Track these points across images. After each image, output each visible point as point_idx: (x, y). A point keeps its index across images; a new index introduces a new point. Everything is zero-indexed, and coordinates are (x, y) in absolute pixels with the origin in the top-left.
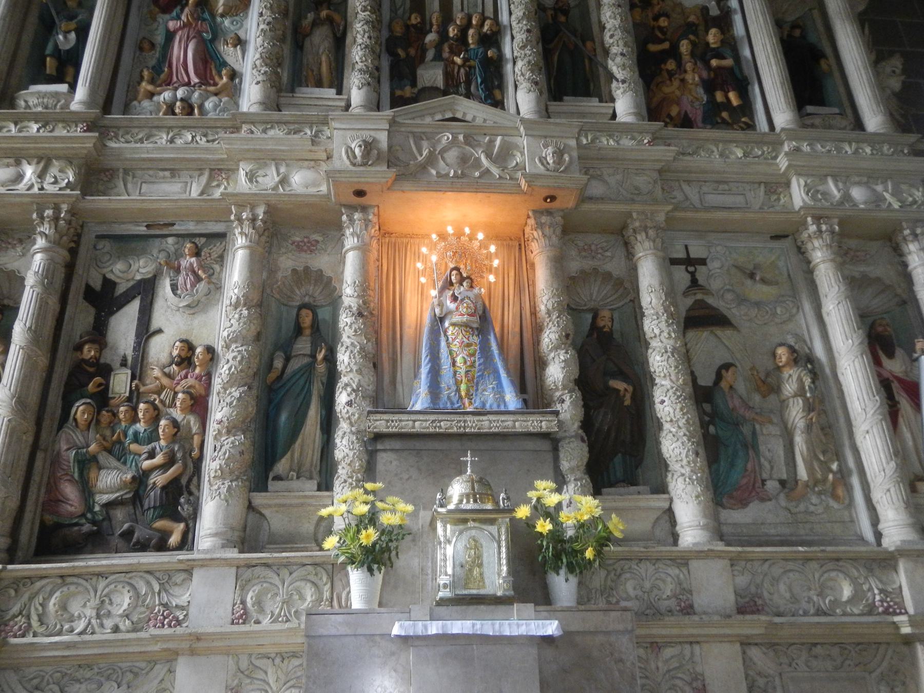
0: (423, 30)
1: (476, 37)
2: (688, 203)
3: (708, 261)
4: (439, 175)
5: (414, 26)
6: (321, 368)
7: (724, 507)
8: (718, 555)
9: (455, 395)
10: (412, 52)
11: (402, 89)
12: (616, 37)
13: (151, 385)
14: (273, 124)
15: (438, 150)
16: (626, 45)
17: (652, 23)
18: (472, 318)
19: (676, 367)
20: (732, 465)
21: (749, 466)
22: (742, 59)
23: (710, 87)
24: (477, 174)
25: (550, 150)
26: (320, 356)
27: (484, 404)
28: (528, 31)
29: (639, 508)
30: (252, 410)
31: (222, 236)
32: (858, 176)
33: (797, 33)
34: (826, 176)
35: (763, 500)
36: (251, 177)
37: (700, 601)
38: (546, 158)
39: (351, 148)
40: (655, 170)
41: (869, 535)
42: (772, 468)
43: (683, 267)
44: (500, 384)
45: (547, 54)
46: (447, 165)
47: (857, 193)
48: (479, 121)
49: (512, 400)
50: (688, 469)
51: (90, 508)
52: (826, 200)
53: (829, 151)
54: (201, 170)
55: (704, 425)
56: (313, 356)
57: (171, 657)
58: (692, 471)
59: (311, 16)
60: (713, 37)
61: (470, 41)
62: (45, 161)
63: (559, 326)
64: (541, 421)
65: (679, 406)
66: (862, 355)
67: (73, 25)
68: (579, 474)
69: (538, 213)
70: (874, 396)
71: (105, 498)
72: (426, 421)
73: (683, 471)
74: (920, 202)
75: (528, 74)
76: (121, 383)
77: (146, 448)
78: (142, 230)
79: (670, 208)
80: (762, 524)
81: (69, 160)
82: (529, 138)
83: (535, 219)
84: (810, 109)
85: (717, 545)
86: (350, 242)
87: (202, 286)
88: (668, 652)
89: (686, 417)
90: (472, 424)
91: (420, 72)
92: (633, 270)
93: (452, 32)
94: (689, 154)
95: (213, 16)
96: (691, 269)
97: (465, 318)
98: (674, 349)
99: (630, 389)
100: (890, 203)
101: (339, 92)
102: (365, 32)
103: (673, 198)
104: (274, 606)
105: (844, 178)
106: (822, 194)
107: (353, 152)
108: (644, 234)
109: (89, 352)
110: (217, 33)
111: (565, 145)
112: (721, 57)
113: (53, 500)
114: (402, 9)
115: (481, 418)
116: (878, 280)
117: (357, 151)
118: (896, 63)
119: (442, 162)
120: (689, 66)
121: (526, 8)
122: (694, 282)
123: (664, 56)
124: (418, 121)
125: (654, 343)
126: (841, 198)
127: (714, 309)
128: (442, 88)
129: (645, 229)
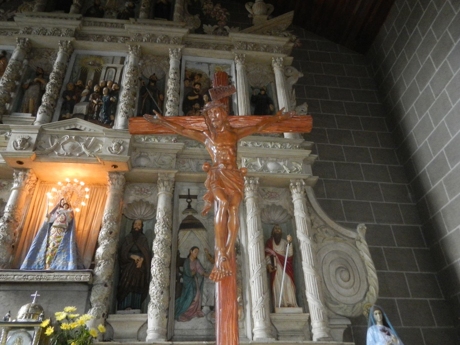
0: (82, 88)
1: (107, 92)
2: (191, 169)
3: (198, 196)
4: (59, 154)
5: (78, 86)
7: (178, 320)
9: (42, 262)
10: (74, 97)
11: (65, 114)
12: (170, 93)
15: (62, 143)
16: (174, 96)
17: (194, 87)
18: (64, 224)
19: (161, 249)
20: (186, 298)
21: (196, 299)
22: (233, 103)
24: (78, 154)
27: (56, 267)
28: (128, 89)
29: (131, 321)
32: (272, 158)
33: (263, 92)
34: (257, 158)
35: (199, 316)
38: (112, 148)
39: (16, 142)
40: (175, 154)
41: (249, 336)
42: (207, 300)
43: (186, 199)
44: (68, 257)
46: (64, 150)
48: (87, 130)
49: (71, 266)
50: (156, 300)
52: (254, 169)
53: (261, 146)
55: (178, 278)
58: (158, 301)
61: (104, 93)
63: (107, 228)
64: (81, 276)
65: (159, 268)
66: (257, 243)
68: (99, 303)
69: (111, 173)
70: (259, 264)
72: (21, 275)
73: (154, 301)
74: (300, 170)
75: (124, 109)
79: (176, 171)
80: (196, 329)
82: (107, 138)
83: (109, 176)
85: (160, 341)
86: (15, 185)
89: (160, 274)
91: (75, 106)
93: (95, 89)
94: (195, 146)
96: (189, 200)
97: (58, 224)
99: (142, 259)
100: (285, 170)
102: (49, 88)
103: (184, 167)
105: (265, 159)
106: (253, 166)
107: (17, 143)
108: (162, 184)
111: (123, 142)
114: (75, 78)
115: (50, 274)
116: (280, 207)
117: (18, 143)
119: (62, 149)
121: (130, 79)
122: (189, 207)
123: (195, 101)
124: (58, 130)
125: (157, 237)
126: (261, 168)
127: (196, 220)
128: (85, 114)
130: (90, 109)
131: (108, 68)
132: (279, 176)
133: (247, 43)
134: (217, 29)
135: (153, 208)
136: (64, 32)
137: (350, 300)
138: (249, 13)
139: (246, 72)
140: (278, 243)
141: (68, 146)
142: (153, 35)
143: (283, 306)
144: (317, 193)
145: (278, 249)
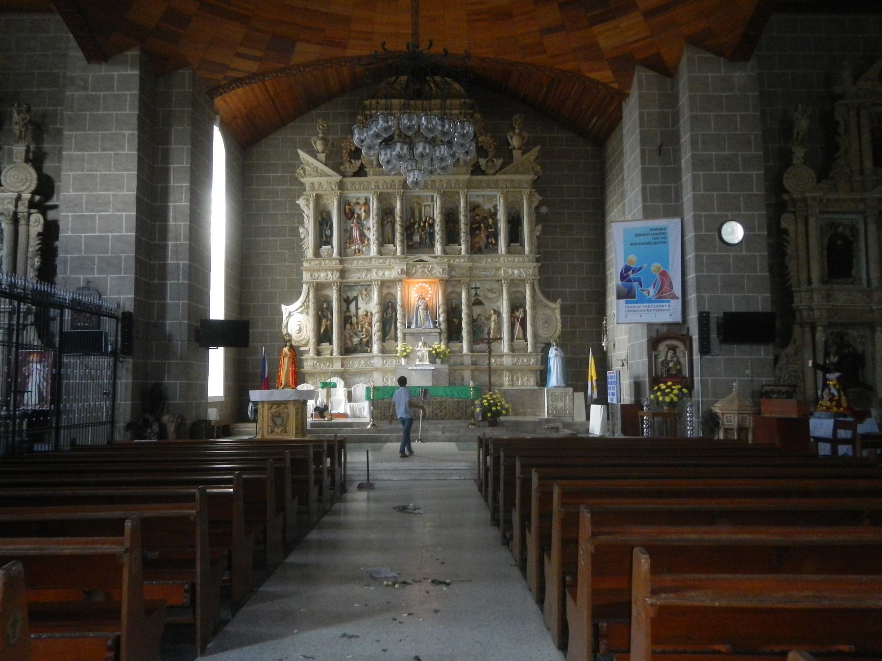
0: (414, 223)
6: (394, 317)
8: (469, 355)
13: (360, 320)
14: (380, 258)
23: (488, 237)
25: (441, 270)
26: (394, 314)
30: (381, 326)
31: (370, 285)
33: (516, 216)
36: (376, 273)
37: (465, 363)
45: (447, 227)
49: (432, 326)
51: (353, 344)
54: (365, 270)
55: (473, 328)
56: (392, 314)
59: (386, 221)
60: (490, 221)
62: (332, 270)
67: (328, 227)
71: (355, 343)
76: (354, 320)
77: (361, 334)
78: (353, 284)
81: (337, 270)
84: (512, 244)
86: (399, 289)
87: (368, 298)
88: (458, 371)
90: (423, 331)
92: (462, 292)
93: (422, 224)
95: (361, 220)
98: (467, 313)
99: (458, 321)
101: (394, 246)
109: (347, 314)
110: (362, 225)
112: (491, 228)
113: (346, 344)
118: (539, 227)
120: (482, 232)
122: (476, 294)
129: (464, 284)
130: (421, 238)
131: (425, 206)
132: (520, 278)
133: (506, 180)
134: (488, 161)
135: (460, 295)
136: (397, 182)
137: (546, 336)
138: (509, 144)
140: (517, 311)
141: (420, 271)
142: (449, 180)
143: (516, 339)
144: (540, 285)
145: (517, 314)
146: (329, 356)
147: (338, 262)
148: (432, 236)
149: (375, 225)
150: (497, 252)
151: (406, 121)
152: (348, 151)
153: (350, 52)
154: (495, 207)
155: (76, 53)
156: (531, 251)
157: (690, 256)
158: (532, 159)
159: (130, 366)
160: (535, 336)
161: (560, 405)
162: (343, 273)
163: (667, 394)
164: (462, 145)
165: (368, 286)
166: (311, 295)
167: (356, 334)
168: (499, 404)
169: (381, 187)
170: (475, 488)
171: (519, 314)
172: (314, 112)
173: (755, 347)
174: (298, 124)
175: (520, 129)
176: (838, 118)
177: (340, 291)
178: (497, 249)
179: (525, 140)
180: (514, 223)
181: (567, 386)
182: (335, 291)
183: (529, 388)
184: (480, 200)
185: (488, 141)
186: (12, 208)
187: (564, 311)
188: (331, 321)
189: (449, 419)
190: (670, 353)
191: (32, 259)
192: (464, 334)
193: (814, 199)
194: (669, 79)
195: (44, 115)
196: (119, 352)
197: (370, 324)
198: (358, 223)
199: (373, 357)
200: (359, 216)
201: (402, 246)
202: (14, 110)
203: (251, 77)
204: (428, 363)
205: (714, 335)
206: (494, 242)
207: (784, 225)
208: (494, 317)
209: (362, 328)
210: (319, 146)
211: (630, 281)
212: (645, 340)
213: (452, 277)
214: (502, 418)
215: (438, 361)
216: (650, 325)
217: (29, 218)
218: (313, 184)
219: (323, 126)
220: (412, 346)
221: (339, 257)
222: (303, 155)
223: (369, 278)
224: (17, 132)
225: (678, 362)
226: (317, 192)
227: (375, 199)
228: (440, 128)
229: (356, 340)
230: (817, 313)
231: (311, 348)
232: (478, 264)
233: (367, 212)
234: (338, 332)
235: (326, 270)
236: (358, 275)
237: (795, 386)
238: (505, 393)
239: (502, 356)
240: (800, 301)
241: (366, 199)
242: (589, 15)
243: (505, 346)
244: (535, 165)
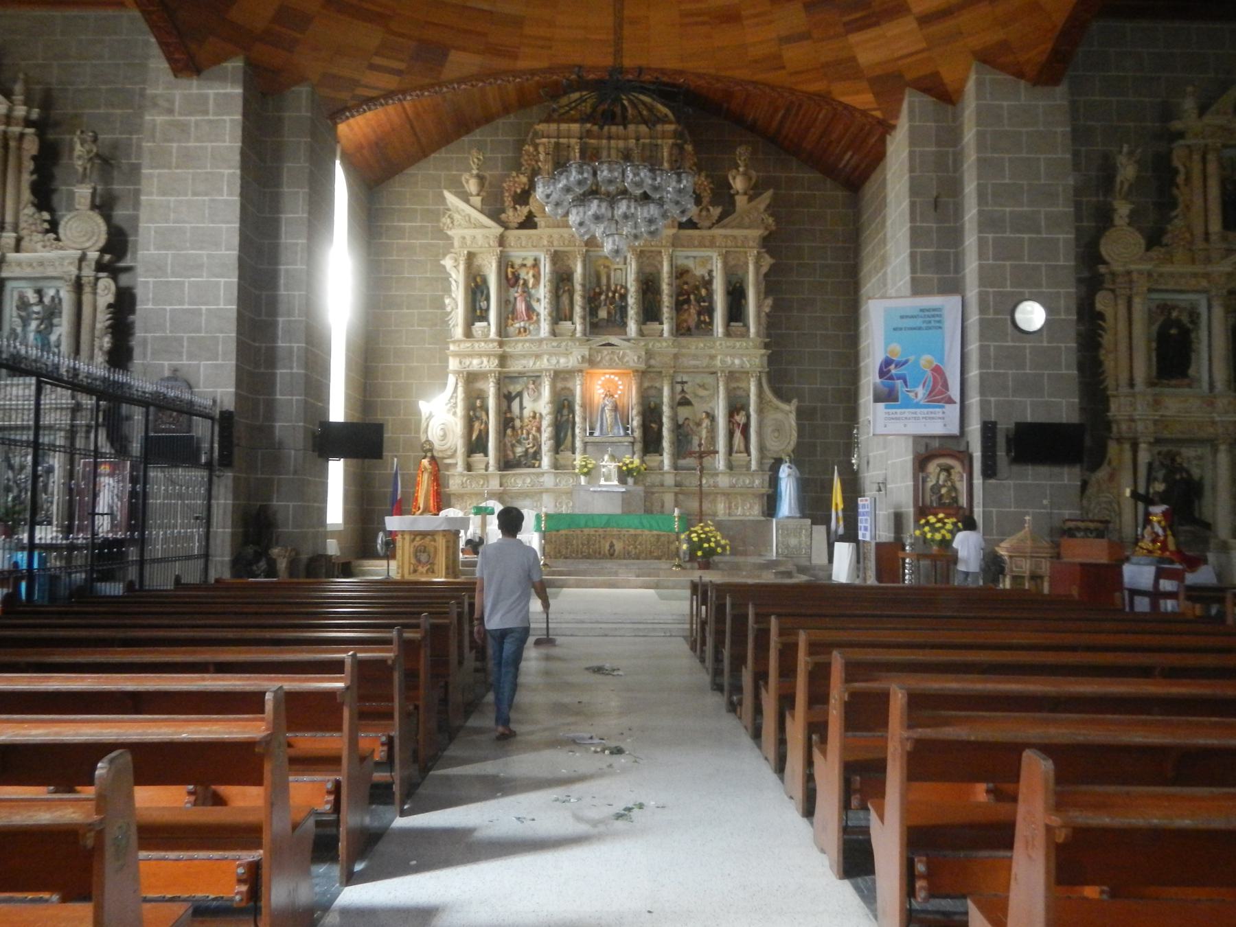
0: (600, 294)
23: (699, 314)
25: (636, 358)
31: (539, 377)
36: (548, 360)
47: (737, 362)
49: (622, 432)
57: (541, 493)
60: (703, 292)
62: (488, 356)
76: (518, 423)
81: (494, 355)
84: (732, 324)
86: (578, 382)
93: (610, 295)
104: (563, 482)
109: (509, 415)
110: (530, 295)
112: (704, 301)
113: (506, 456)
118: (769, 301)
122: (683, 391)
130: (609, 313)
131: (615, 270)
133: (726, 237)
134: (701, 211)
135: (660, 391)
138: (730, 187)
139: (725, 264)
141: (607, 358)
144: (770, 381)
145: (737, 418)
146: (483, 472)
147: (496, 344)
148: (623, 310)
149: (547, 295)
150: (712, 335)
151: (605, 173)
152: (512, 193)
153: (522, 64)
154: (710, 272)
155: (159, 64)
156: (758, 334)
157: (974, 347)
158: (762, 207)
159: (230, 483)
160: (762, 449)
161: (793, 541)
162: (503, 359)
163: (938, 530)
164: (677, 203)
165: (536, 378)
166: (460, 389)
167: (519, 442)
168: (713, 539)
169: (555, 243)
170: (686, 647)
171: (740, 419)
172: (465, 139)
173: (1056, 470)
174: (443, 155)
175: (746, 166)
176: (1176, 163)
177: (499, 384)
178: (712, 330)
179: (754, 180)
180: (736, 295)
181: (804, 516)
182: (492, 384)
183: (751, 518)
184: (690, 264)
185: (702, 184)
186: (74, 271)
187: (800, 414)
188: (487, 424)
189: (646, 559)
190: (943, 476)
191: (101, 338)
192: (666, 444)
193: (1140, 272)
194: (950, 107)
195: (115, 146)
196: (215, 462)
197: (539, 430)
198: (524, 292)
199: (543, 474)
200: (525, 283)
201: (584, 324)
202: (76, 139)
203: (388, 95)
204: (616, 483)
205: (1001, 453)
206: (707, 320)
207: (1099, 306)
208: (706, 422)
209: (528, 434)
210: (472, 186)
211: (891, 378)
212: (909, 458)
213: (650, 367)
214: (716, 558)
215: (630, 480)
216: (917, 439)
217: (96, 284)
218: (464, 238)
219: (478, 159)
220: (595, 460)
221: (498, 338)
222: (451, 199)
223: (538, 365)
224: (80, 170)
225: (954, 488)
226: (471, 250)
227: (548, 260)
228: (650, 182)
229: (519, 450)
230: (1140, 427)
231: (460, 460)
232: (684, 351)
233: (537, 277)
234: (496, 439)
235: (480, 355)
236: (524, 362)
237: (1107, 522)
238: (719, 526)
239: (717, 475)
240: (1118, 409)
241: (535, 260)
242: (846, 19)
243: (720, 462)
244: (765, 216)
